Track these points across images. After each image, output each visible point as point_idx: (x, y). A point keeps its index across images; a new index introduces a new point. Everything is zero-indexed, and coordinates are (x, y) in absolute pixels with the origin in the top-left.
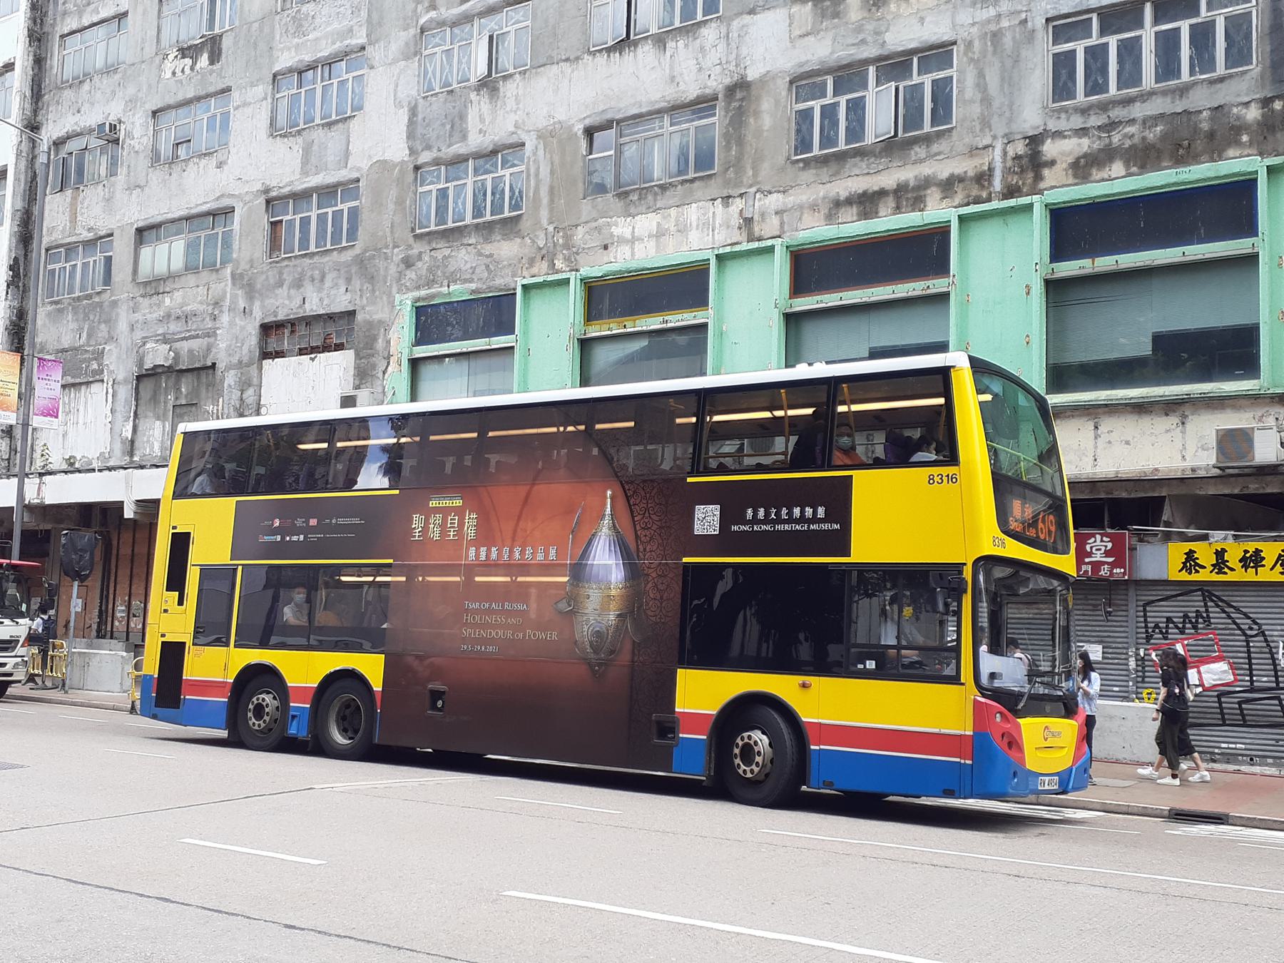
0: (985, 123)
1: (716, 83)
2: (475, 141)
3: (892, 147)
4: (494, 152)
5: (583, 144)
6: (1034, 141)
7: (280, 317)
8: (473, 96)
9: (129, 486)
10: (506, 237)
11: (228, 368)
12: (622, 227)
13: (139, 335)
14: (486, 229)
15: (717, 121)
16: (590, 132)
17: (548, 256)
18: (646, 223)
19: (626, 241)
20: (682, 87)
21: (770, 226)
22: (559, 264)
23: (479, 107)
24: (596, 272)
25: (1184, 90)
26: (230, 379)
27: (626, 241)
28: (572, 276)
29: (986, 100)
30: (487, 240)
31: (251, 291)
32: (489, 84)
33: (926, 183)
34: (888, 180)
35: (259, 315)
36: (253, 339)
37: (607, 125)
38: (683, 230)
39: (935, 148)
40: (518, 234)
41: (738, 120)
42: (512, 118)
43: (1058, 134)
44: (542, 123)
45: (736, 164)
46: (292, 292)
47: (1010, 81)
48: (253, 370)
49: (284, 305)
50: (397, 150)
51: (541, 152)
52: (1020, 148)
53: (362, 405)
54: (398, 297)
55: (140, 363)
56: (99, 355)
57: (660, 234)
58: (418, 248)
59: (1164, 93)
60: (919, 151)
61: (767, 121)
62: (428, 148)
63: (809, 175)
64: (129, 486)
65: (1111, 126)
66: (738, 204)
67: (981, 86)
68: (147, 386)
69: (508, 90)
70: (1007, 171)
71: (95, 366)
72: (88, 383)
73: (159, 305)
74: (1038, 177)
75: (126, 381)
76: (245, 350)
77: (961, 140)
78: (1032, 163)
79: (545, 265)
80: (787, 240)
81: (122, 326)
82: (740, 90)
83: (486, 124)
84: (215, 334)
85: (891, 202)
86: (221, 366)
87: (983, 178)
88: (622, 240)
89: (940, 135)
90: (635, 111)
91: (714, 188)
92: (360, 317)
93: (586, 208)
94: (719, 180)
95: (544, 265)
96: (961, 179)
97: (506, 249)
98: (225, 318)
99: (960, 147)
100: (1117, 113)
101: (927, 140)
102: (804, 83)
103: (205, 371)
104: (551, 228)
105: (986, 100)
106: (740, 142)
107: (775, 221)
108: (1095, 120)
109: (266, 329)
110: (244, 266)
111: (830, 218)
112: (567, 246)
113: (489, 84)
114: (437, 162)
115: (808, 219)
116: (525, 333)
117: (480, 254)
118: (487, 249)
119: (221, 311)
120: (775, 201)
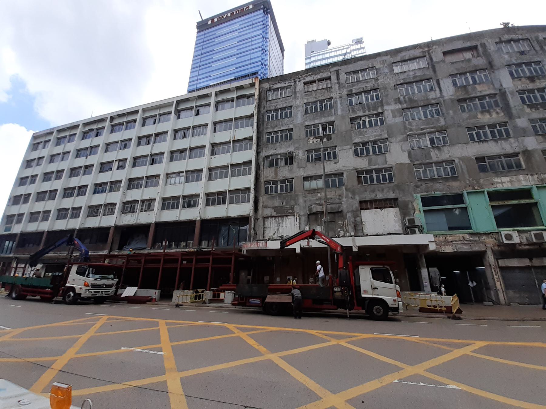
2: (435, 159)
4: (443, 162)
7: (367, 199)
8: (432, 150)
9: (354, 241)
11: (348, 212)
12: (497, 180)
13: (308, 204)
18: (505, 179)
19: (500, 183)
20: (507, 150)
24: (490, 190)
26: (349, 215)
27: (500, 183)
31: (354, 193)
35: (358, 198)
36: (357, 205)
40: (458, 180)
46: (371, 193)
48: (359, 213)
49: (368, 196)
50: (405, 160)
51: (461, 162)
53: (426, 219)
54: (415, 195)
55: (310, 210)
56: (293, 209)
57: (511, 182)
58: (419, 183)
62: (418, 160)
64: (354, 241)
68: (313, 217)
71: (291, 211)
72: (286, 216)
73: (316, 196)
75: (304, 215)
76: (354, 207)
81: (301, 201)
84: (341, 203)
86: (345, 211)
92: (400, 199)
93: (482, 174)
95: (471, 188)
97: (455, 184)
98: (344, 199)
103: (337, 214)
104: (471, 179)
109: (361, 202)
110: (349, 187)
112: (478, 182)
114: (421, 164)
117: (445, 185)
119: (342, 198)
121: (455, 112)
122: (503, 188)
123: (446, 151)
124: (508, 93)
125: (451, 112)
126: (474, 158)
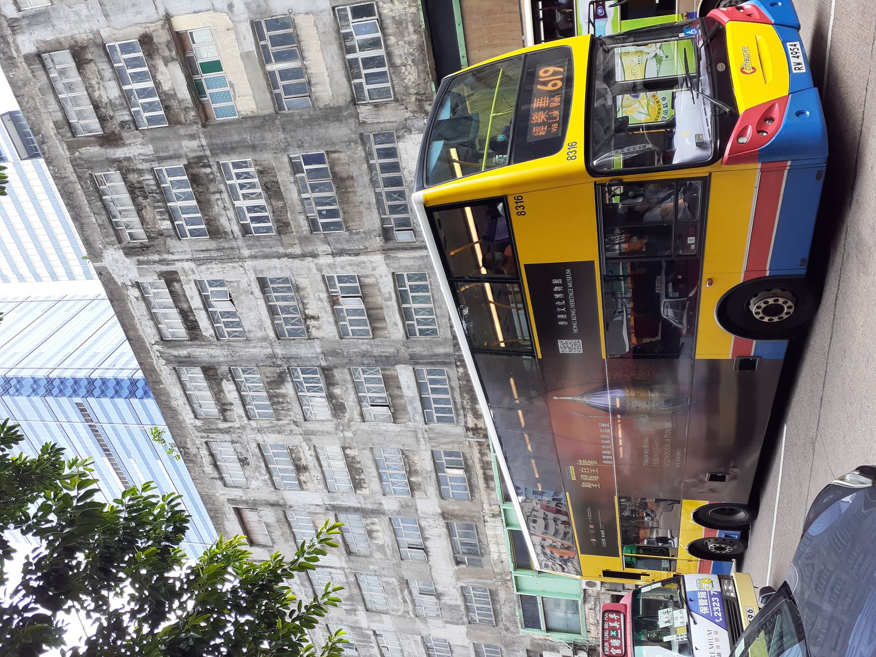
0: (461, 443)
1: (442, 522)
2: (460, 602)
3: (467, 469)
4: (464, 596)
5: (462, 566)
6: (468, 429)
10: (497, 595)
12: (494, 556)
14: (494, 601)
15: (455, 524)
16: (458, 563)
17: (505, 582)
18: (493, 548)
21: (496, 509)
22: (509, 578)
23: (446, 600)
25: (452, 388)
28: (513, 575)
29: (453, 442)
30: (499, 602)
32: (438, 596)
33: (481, 461)
34: (480, 472)
37: (456, 558)
38: (496, 536)
39: (469, 457)
40: (496, 591)
41: (455, 516)
42: (451, 589)
43: (466, 423)
44: (454, 580)
45: (472, 518)
47: (446, 435)
52: (470, 434)
57: (497, 543)
59: (453, 393)
60: (470, 462)
61: (457, 507)
63: (477, 495)
65: (464, 408)
66: (487, 518)
67: (448, 443)
69: (440, 589)
70: (478, 437)
74: (481, 429)
77: (466, 450)
78: (476, 430)
79: (509, 583)
80: (501, 504)
82: (444, 515)
83: (453, 597)
85: (488, 471)
87: (480, 444)
88: (499, 556)
89: (464, 456)
90: (450, 549)
91: (481, 526)
94: (478, 524)
96: (481, 450)
97: (502, 595)
99: (469, 450)
100: (459, 406)
101: (466, 460)
102: (442, 496)
105: (453, 442)
106: (463, 516)
107: (493, 507)
108: (461, 412)
111: (493, 489)
112: (501, 574)
113: (438, 596)
115: (493, 496)
116: (536, 591)
118: (502, 602)
120: (486, 506)
121: (372, 564)
122: (509, 553)
123: (446, 589)
124: (332, 503)
125: (371, 567)
126: (456, 567)
